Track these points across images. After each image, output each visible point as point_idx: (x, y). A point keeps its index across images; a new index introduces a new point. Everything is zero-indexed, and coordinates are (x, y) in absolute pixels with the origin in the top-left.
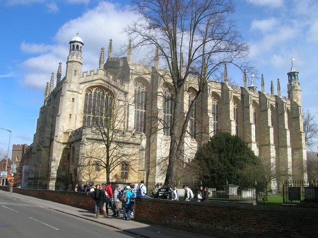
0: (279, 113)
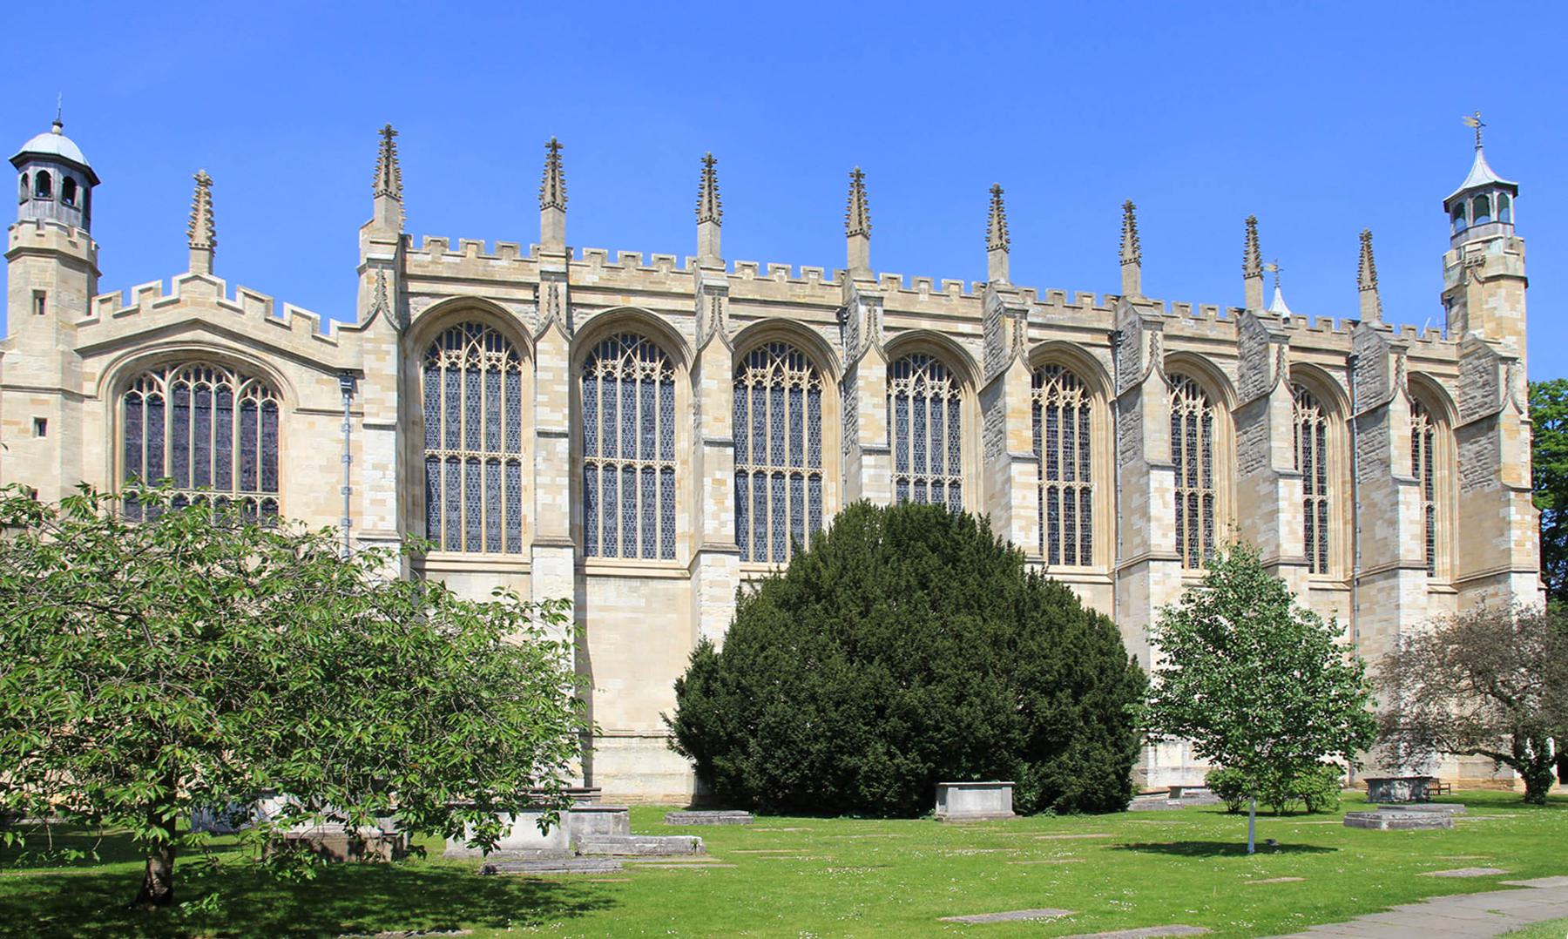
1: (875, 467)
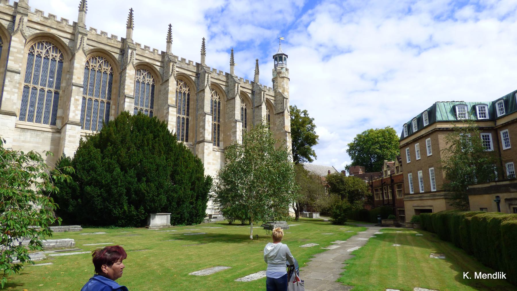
0: (256, 106)
1: (129, 102)
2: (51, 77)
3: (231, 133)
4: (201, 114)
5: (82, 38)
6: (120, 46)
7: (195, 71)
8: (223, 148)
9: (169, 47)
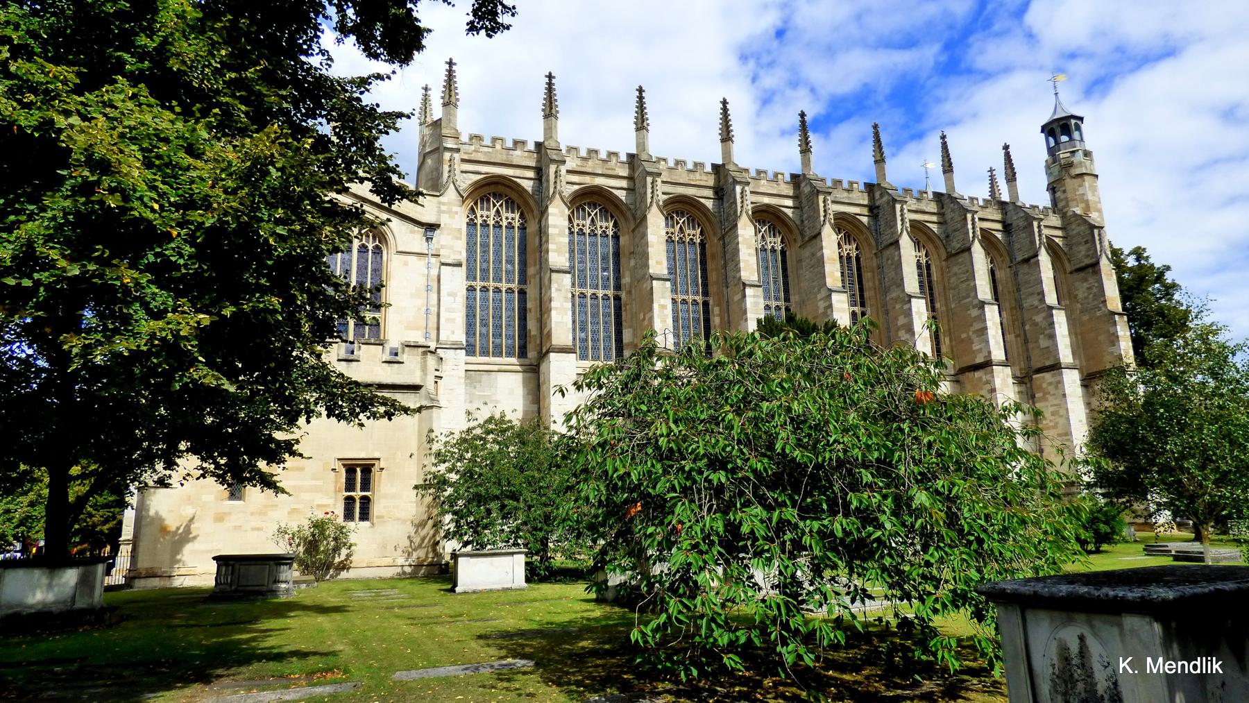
0: (1019, 258)
2: (604, 270)
3: (971, 333)
4: (896, 300)
5: (652, 183)
6: (711, 183)
7: (866, 202)
8: (952, 373)
9: (806, 163)
